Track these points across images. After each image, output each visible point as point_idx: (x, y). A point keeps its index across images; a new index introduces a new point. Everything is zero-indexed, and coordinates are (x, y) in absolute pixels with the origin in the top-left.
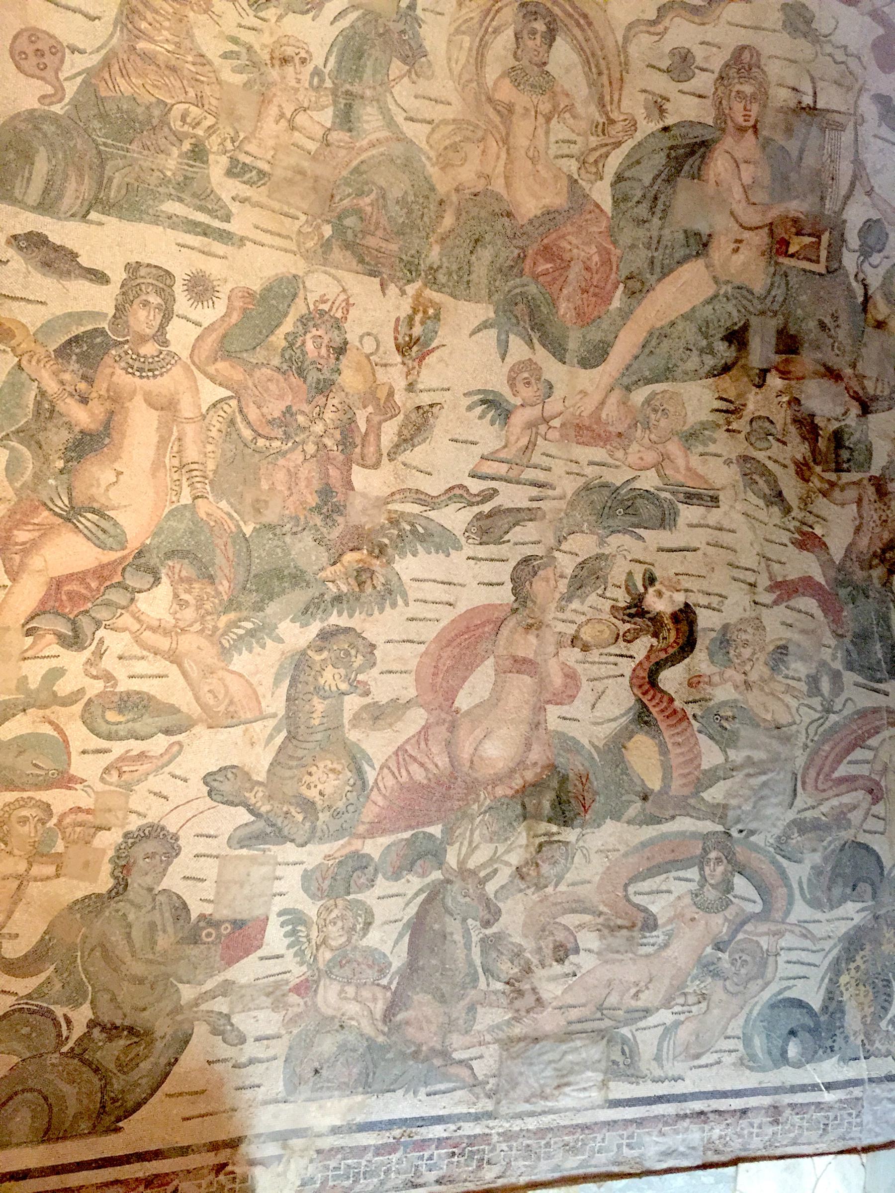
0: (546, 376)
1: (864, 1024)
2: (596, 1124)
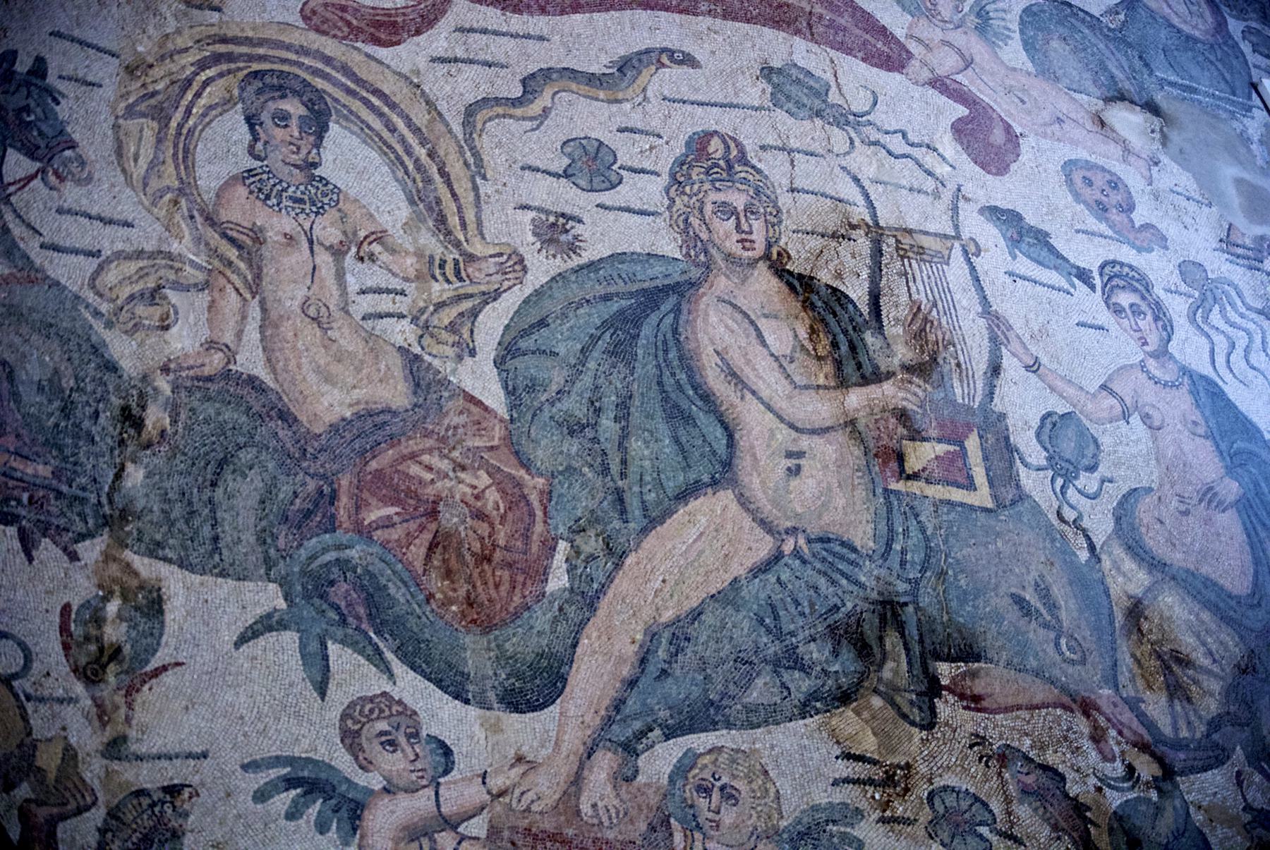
0: (430, 728)
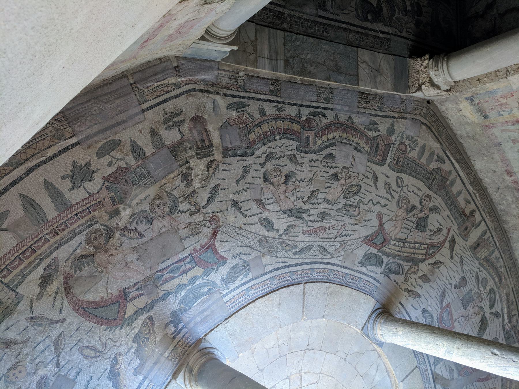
1: (389, 16)
2: (315, 21)
